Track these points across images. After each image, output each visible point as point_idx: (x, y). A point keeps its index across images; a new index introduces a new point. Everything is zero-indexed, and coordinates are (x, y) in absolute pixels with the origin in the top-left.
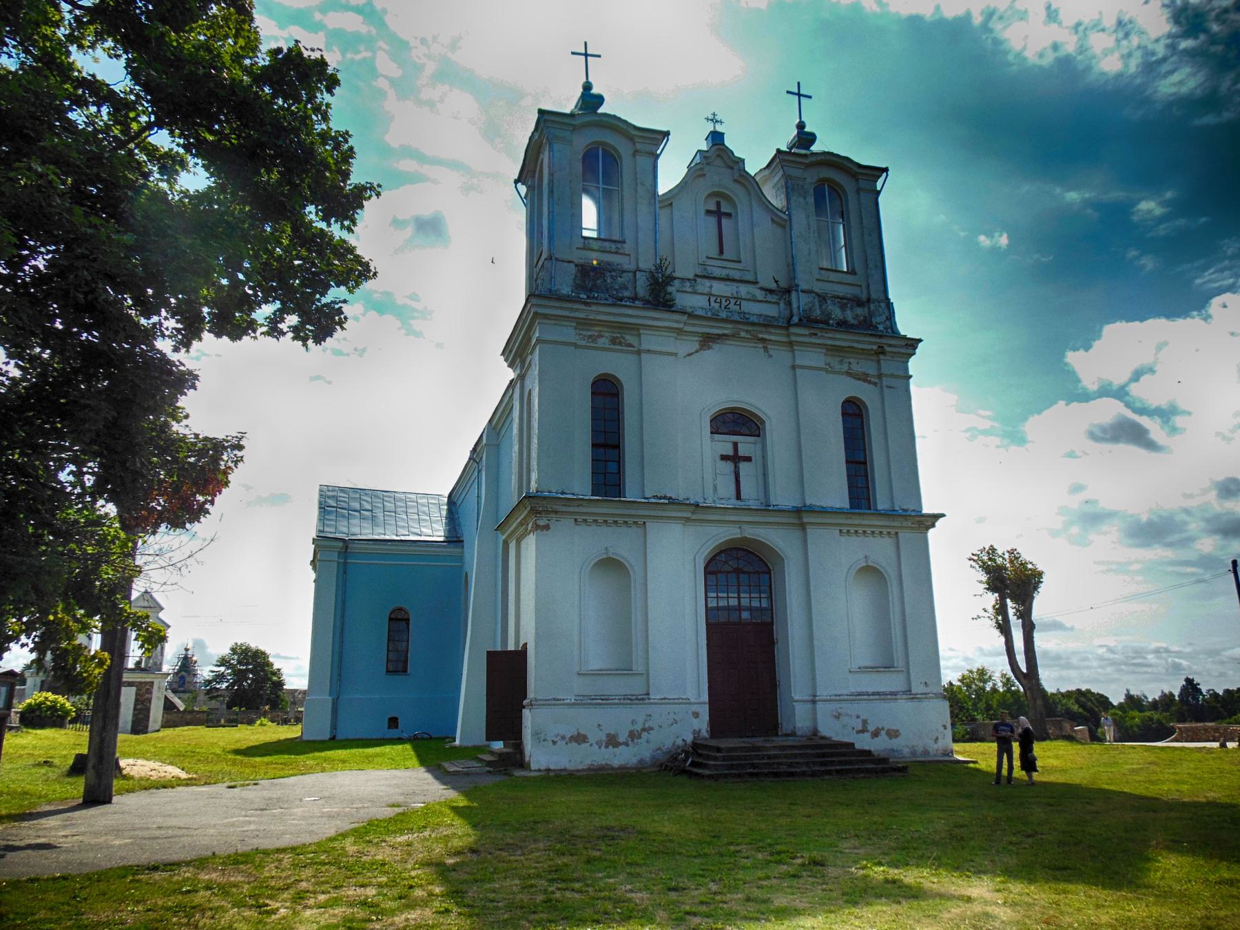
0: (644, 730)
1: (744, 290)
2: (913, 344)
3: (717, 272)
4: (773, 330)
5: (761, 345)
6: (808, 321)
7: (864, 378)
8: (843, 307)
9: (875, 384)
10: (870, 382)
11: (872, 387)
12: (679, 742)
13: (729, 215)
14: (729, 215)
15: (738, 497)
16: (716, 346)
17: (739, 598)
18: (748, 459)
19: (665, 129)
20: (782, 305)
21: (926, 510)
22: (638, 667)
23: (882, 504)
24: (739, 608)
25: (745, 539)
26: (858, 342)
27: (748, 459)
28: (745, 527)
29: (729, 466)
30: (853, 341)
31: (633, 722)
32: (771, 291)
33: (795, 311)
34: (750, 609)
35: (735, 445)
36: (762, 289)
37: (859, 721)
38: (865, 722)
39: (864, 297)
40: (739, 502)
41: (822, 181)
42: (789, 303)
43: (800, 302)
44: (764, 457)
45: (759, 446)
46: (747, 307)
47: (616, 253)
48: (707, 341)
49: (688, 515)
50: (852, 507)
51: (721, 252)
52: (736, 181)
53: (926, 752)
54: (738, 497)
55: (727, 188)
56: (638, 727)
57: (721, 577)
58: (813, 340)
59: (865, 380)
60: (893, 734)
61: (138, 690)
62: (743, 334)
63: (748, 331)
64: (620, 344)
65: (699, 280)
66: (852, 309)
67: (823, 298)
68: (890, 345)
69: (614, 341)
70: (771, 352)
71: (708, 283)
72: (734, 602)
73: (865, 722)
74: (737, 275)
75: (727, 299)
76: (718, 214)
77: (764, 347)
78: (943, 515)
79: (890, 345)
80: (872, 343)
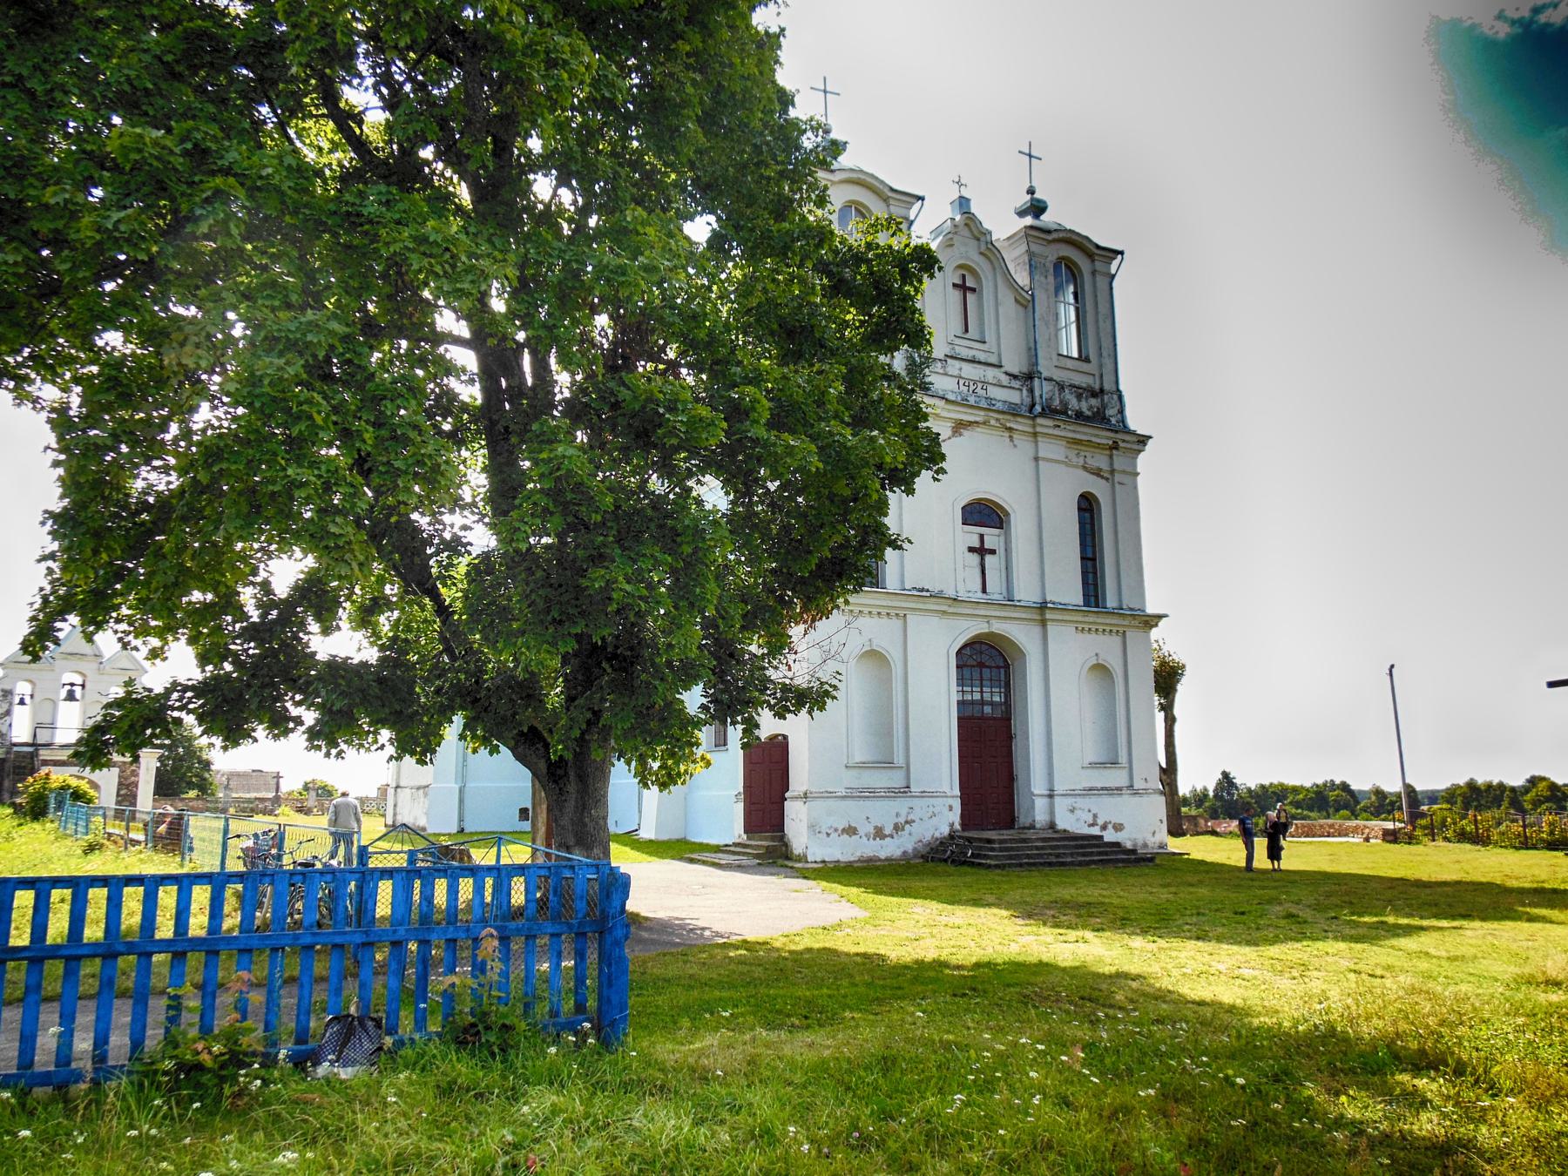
0: (907, 822)
1: (991, 374)
2: (1143, 440)
3: (965, 353)
4: (1019, 419)
5: (1007, 434)
6: (1049, 411)
7: (1097, 473)
8: (1079, 397)
9: (1107, 479)
10: (1102, 477)
11: (1104, 481)
12: (937, 835)
13: (973, 290)
14: (973, 290)
15: (984, 590)
16: (965, 432)
17: (982, 692)
18: (993, 552)
19: (920, 194)
21: (1150, 610)
22: (899, 760)
23: (1111, 602)
24: (982, 702)
25: (992, 635)
26: (1097, 436)
27: (993, 552)
28: (993, 621)
29: (975, 558)
30: (1092, 435)
31: (897, 815)
32: (1015, 377)
33: (1037, 399)
34: (992, 703)
35: (982, 537)
36: (1006, 373)
37: (1091, 815)
38: (1095, 816)
39: (1097, 387)
40: (984, 596)
41: (1063, 258)
42: (1031, 391)
43: (1043, 390)
44: (1008, 551)
45: (1002, 539)
46: (995, 393)
49: (944, 608)
50: (1086, 604)
52: (981, 253)
53: (1145, 845)
54: (984, 590)
55: (973, 261)
56: (902, 820)
57: (986, 672)
58: (1056, 432)
59: (1098, 475)
60: (1118, 828)
61: (122, 771)
62: (993, 422)
63: (997, 420)
65: (949, 360)
66: (1087, 399)
67: (1061, 387)
68: (1124, 441)
70: (1016, 442)
71: (957, 364)
72: (977, 696)
73: (1095, 816)
74: (982, 357)
76: (962, 287)
77: (1011, 437)
78: (1166, 616)
79: (1124, 441)
80: (1108, 438)
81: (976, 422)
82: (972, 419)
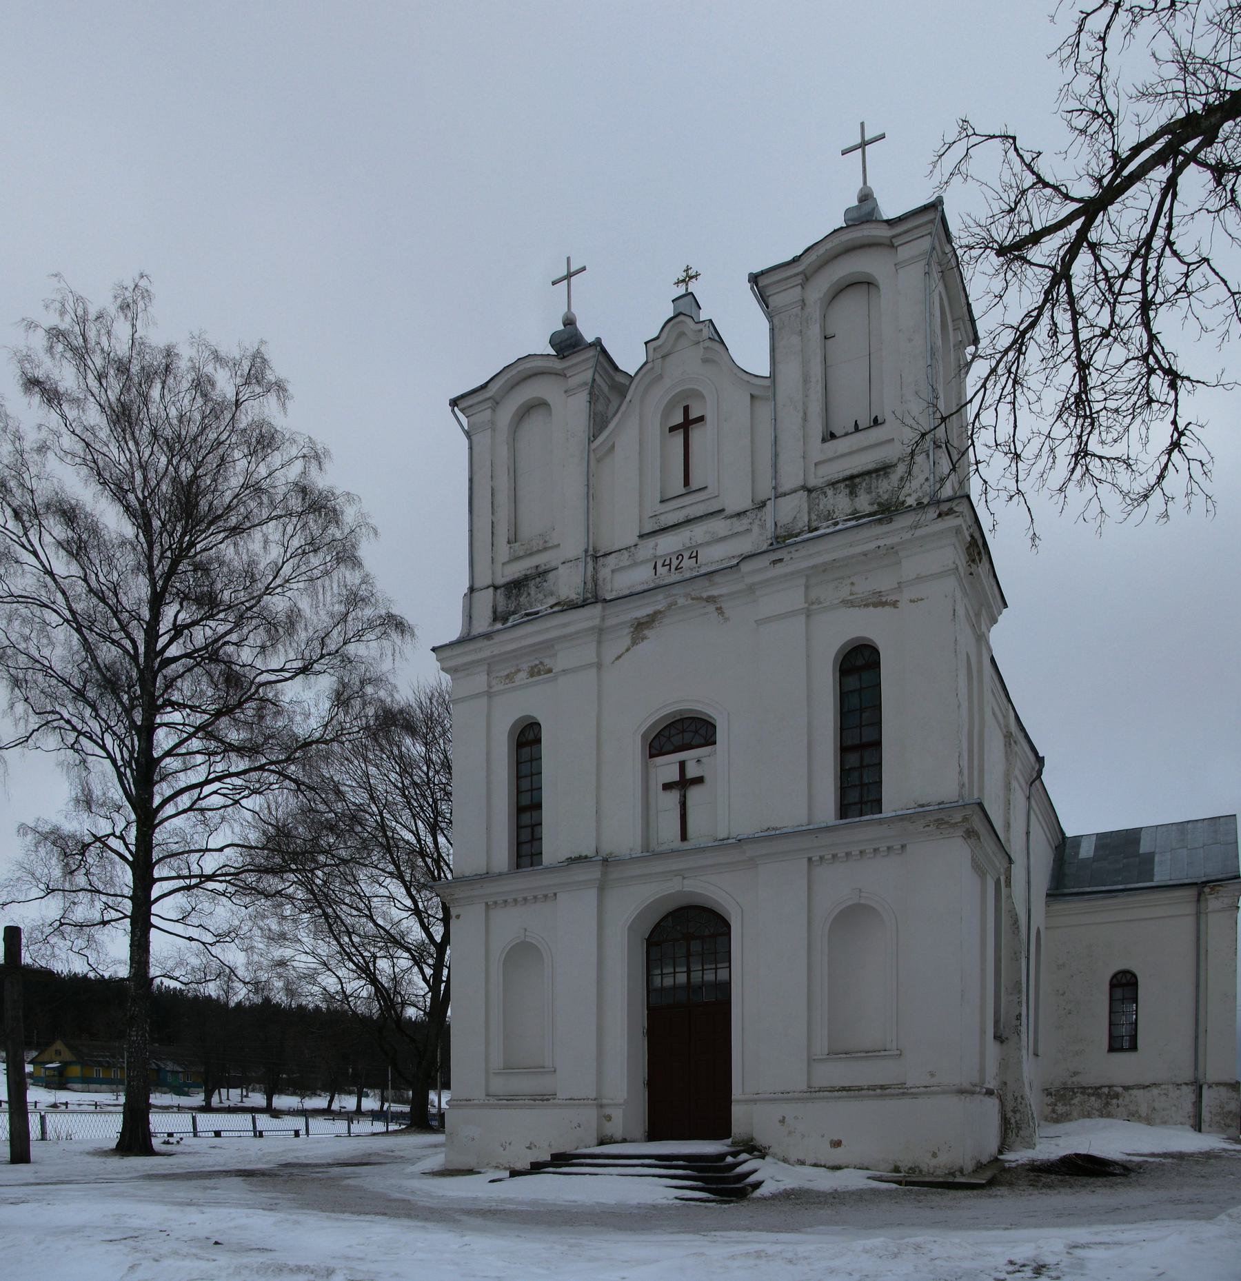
1: (699, 532)
15: (684, 837)
18: (699, 780)
20: (756, 529)
27: (699, 780)
29: (674, 796)
35: (682, 765)
47: (545, 549)
48: (641, 627)
51: (687, 482)
54: (684, 837)
58: (780, 569)
62: (681, 601)
64: (539, 673)
69: (533, 673)
71: (651, 542)
72: (682, 978)
75: (680, 556)
77: (719, 609)
81: (656, 613)
82: (649, 610)
